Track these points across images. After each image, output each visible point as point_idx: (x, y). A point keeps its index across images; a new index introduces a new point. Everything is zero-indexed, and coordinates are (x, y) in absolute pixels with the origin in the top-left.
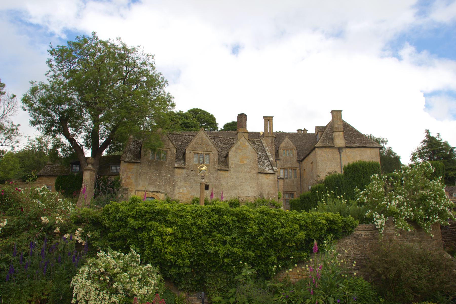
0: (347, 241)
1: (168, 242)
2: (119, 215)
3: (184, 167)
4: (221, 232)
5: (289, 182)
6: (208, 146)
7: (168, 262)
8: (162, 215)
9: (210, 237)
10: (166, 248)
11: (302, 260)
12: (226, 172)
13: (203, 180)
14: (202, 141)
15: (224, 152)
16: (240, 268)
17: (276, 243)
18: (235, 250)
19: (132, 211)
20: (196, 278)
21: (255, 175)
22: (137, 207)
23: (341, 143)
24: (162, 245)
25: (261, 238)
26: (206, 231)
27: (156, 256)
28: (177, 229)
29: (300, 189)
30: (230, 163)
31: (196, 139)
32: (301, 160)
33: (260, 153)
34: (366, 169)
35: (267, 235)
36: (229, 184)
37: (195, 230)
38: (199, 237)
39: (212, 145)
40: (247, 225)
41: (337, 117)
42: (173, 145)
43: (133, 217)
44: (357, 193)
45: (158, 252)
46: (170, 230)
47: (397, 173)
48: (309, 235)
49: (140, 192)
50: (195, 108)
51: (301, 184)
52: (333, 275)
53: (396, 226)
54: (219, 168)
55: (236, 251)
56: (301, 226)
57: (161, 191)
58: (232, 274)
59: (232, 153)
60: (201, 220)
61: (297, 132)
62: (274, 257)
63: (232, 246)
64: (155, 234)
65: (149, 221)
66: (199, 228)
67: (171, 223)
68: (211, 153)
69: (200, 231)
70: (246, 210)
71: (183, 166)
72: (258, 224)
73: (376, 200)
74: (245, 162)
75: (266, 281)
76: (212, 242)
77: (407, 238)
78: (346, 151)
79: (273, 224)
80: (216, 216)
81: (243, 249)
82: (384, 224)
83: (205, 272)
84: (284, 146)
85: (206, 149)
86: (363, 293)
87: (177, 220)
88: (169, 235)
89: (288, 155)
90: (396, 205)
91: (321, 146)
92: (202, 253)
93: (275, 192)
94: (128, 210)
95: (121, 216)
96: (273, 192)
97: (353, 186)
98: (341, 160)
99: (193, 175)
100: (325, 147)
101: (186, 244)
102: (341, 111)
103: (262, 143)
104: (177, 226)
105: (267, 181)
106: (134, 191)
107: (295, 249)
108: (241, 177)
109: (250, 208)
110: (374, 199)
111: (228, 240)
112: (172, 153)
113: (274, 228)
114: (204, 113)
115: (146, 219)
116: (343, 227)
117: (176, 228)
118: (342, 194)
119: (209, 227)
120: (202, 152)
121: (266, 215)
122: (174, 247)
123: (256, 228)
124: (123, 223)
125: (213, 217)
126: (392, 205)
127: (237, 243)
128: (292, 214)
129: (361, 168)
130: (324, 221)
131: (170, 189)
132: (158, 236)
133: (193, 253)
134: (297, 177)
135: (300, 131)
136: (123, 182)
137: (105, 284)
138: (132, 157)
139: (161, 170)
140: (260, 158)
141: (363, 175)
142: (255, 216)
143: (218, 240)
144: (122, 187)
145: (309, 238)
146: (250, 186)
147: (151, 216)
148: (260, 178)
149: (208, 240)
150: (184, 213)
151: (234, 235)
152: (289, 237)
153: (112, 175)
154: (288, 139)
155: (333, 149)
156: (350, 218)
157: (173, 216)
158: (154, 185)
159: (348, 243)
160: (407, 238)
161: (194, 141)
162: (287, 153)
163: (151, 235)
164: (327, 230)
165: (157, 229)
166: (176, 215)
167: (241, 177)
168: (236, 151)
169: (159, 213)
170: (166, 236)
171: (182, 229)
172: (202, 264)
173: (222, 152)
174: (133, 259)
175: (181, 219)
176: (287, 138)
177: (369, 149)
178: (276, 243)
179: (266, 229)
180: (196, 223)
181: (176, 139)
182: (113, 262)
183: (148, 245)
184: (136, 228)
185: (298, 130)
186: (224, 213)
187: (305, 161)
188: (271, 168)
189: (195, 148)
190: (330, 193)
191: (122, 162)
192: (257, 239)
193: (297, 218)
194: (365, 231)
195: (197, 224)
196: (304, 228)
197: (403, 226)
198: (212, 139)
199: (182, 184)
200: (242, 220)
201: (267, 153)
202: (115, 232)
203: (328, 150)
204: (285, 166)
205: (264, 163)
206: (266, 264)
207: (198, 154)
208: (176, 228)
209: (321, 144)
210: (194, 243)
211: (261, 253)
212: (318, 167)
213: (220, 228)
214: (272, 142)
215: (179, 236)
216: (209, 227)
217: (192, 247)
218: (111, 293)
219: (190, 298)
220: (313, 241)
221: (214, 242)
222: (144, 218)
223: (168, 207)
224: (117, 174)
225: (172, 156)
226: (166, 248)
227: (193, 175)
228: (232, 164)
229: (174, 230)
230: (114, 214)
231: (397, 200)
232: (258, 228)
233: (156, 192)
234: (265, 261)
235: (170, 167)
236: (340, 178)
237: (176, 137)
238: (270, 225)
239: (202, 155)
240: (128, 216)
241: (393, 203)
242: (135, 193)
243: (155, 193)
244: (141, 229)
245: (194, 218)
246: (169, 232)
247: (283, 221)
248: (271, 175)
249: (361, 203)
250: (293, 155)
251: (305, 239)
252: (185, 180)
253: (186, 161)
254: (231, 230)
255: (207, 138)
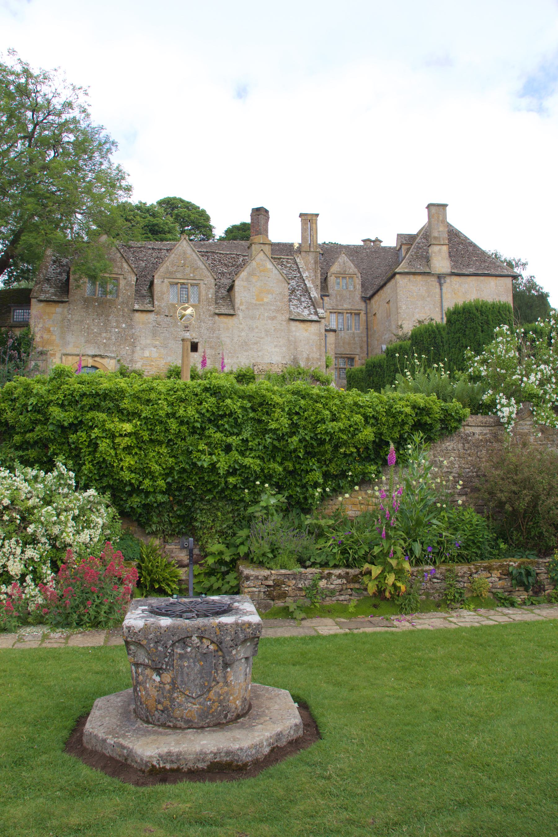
0: (449, 444)
1: (124, 449)
2: (33, 400)
3: (152, 309)
4: (221, 429)
5: (347, 337)
6: (195, 269)
7: (126, 485)
8: (112, 400)
9: (201, 439)
10: (121, 460)
11: (367, 479)
12: (230, 317)
13: (188, 334)
14: (185, 259)
15: (226, 281)
16: (256, 494)
17: (322, 449)
18: (248, 461)
19: (55, 393)
20: (178, 512)
21: (284, 323)
22: (66, 386)
23: (443, 267)
24: (113, 454)
25: (295, 439)
26: (194, 427)
27: (104, 475)
28: (141, 425)
29: (365, 350)
30: (237, 301)
31: (173, 255)
32: (368, 296)
33: (293, 283)
34: (487, 316)
35: (306, 434)
36: (235, 340)
37: (173, 425)
38: (182, 439)
39: (203, 267)
40: (270, 415)
41: (438, 218)
42: (129, 269)
43: (58, 404)
44: (469, 358)
45: (107, 466)
46: (128, 427)
47: (542, 325)
48: (381, 434)
49: (70, 358)
50: (171, 196)
51: (367, 341)
52: (422, 504)
53: (535, 418)
54: (217, 311)
55: (248, 464)
56: (366, 418)
57: (110, 355)
58: (242, 504)
59: (242, 282)
60: (184, 407)
61: (362, 244)
62: (317, 474)
63: (242, 454)
64: (100, 435)
65: (88, 412)
66: (182, 423)
67: (128, 414)
68: (201, 282)
69: (184, 428)
70: (267, 389)
71: (149, 307)
72: (288, 414)
73: (503, 371)
74: (265, 300)
75: (302, 515)
76: (206, 447)
77: (553, 441)
78: (451, 281)
79: (317, 414)
80: (213, 400)
81: (262, 459)
82: (514, 416)
83: (193, 500)
84: (338, 270)
85: (191, 275)
86: (473, 535)
87: (140, 407)
88: (126, 435)
89: (344, 287)
90: (537, 382)
91: (406, 271)
92: (187, 467)
93: (320, 355)
94: (49, 391)
95: (36, 404)
96: (317, 355)
97: (462, 346)
98: (441, 297)
99: (168, 325)
100: (414, 274)
101: (159, 452)
102: (446, 205)
103: (297, 265)
104: (140, 419)
105: (306, 334)
106: (58, 355)
107: (355, 459)
108: (257, 327)
109: (274, 385)
110: (498, 370)
111: (234, 444)
112: (128, 284)
113: (318, 422)
114: (189, 206)
115: (82, 408)
116: (442, 421)
117: (139, 423)
118: (442, 360)
119: (200, 420)
120: (185, 281)
121: (303, 398)
122: (136, 458)
123: (285, 421)
124: (39, 417)
125: (206, 401)
126: (530, 381)
127: (251, 449)
128: (352, 396)
129: (478, 314)
130: (408, 410)
131: (125, 350)
132: (106, 438)
133: (170, 468)
134: (361, 327)
135: (369, 242)
136: (38, 339)
137: (12, 528)
138: (52, 290)
139: (109, 316)
140: (293, 291)
141: (482, 327)
142: (284, 399)
143: (217, 444)
144: (35, 348)
145: (381, 440)
146: (275, 343)
147: (91, 401)
148: (294, 329)
149: (198, 445)
150: (153, 396)
151: (246, 435)
152: (345, 437)
153: (16, 327)
154: (346, 258)
155: (428, 277)
156: (455, 404)
157: (133, 401)
158: (96, 343)
159: (450, 448)
160: (553, 441)
161: (170, 260)
162: (343, 282)
163: (93, 436)
164: (413, 426)
165: (104, 425)
166: (139, 398)
167: (257, 327)
168: (248, 280)
169: (105, 396)
170: (121, 438)
171: (151, 425)
172: (188, 488)
173: (222, 281)
174: (62, 482)
175: (148, 405)
176: (343, 255)
177: (494, 278)
178: (322, 449)
179: (303, 423)
180: (175, 413)
181: (135, 257)
182: (25, 487)
183: (89, 455)
184: (66, 424)
185: (364, 241)
186: (227, 395)
187: (376, 297)
188: (313, 311)
189: (171, 273)
190: (419, 358)
191: (33, 301)
192: (287, 440)
193: (360, 403)
194: (481, 428)
195: (177, 415)
196: (372, 421)
197: (548, 418)
198: (203, 256)
199: (148, 342)
200: (259, 407)
201: (306, 282)
202: (26, 432)
203: (419, 278)
204: (340, 307)
205: (301, 302)
206: (304, 486)
207: (177, 284)
208: (139, 423)
209: (406, 268)
210: (172, 450)
211: (294, 466)
212: (399, 311)
213: (220, 422)
214: (316, 263)
215: (145, 438)
216: (200, 420)
217: (170, 457)
218: (25, 544)
219: (168, 547)
220: (388, 444)
221: (209, 447)
222: (79, 406)
223: (122, 385)
224: (26, 324)
225: (128, 288)
226: (121, 460)
227: (168, 325)
228: (241, 304)
229: (136, 426)
230: (22, 400)
231: (539, 373)
232: (289, 422)
233: (101, 356)
234: (301, 480)
235: (126, 310)
236: (439, 331)
237: (134, 252)
238: (311, 415)
239: (184, 286)
240: (49, 403)
241: (532, 377)
242: (61, 358)
243: (97, 359)
244: (75, 427)
245: (171, 404)
246: (125, 430)
247: (334, 408)
248: (313, 323)
249: (475, 378)
250: (354, 287)
251: (374, 442)
252: (154, 334)
253: (155, 297)
254: (239, 425)
255: (194, 255)
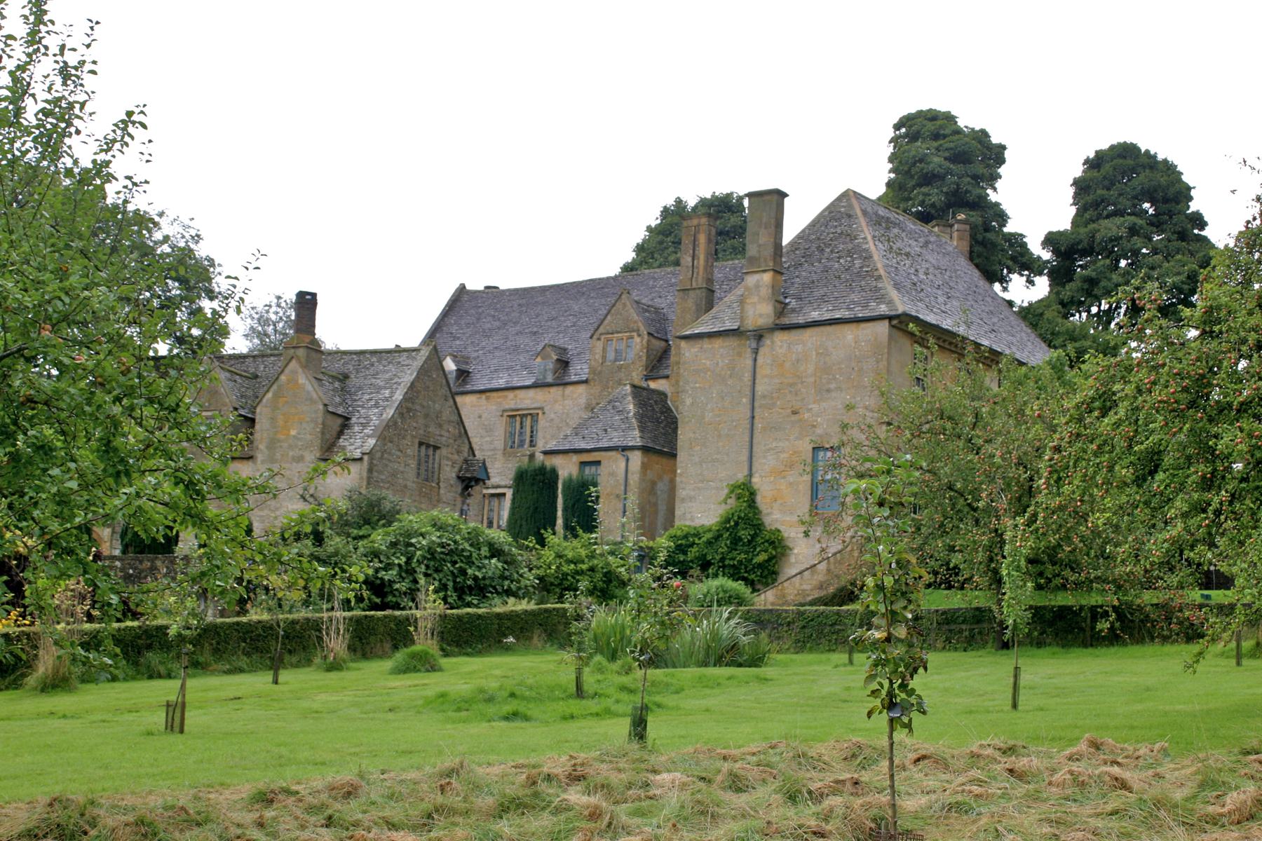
23: (761, 315)
177: (853, 326)
